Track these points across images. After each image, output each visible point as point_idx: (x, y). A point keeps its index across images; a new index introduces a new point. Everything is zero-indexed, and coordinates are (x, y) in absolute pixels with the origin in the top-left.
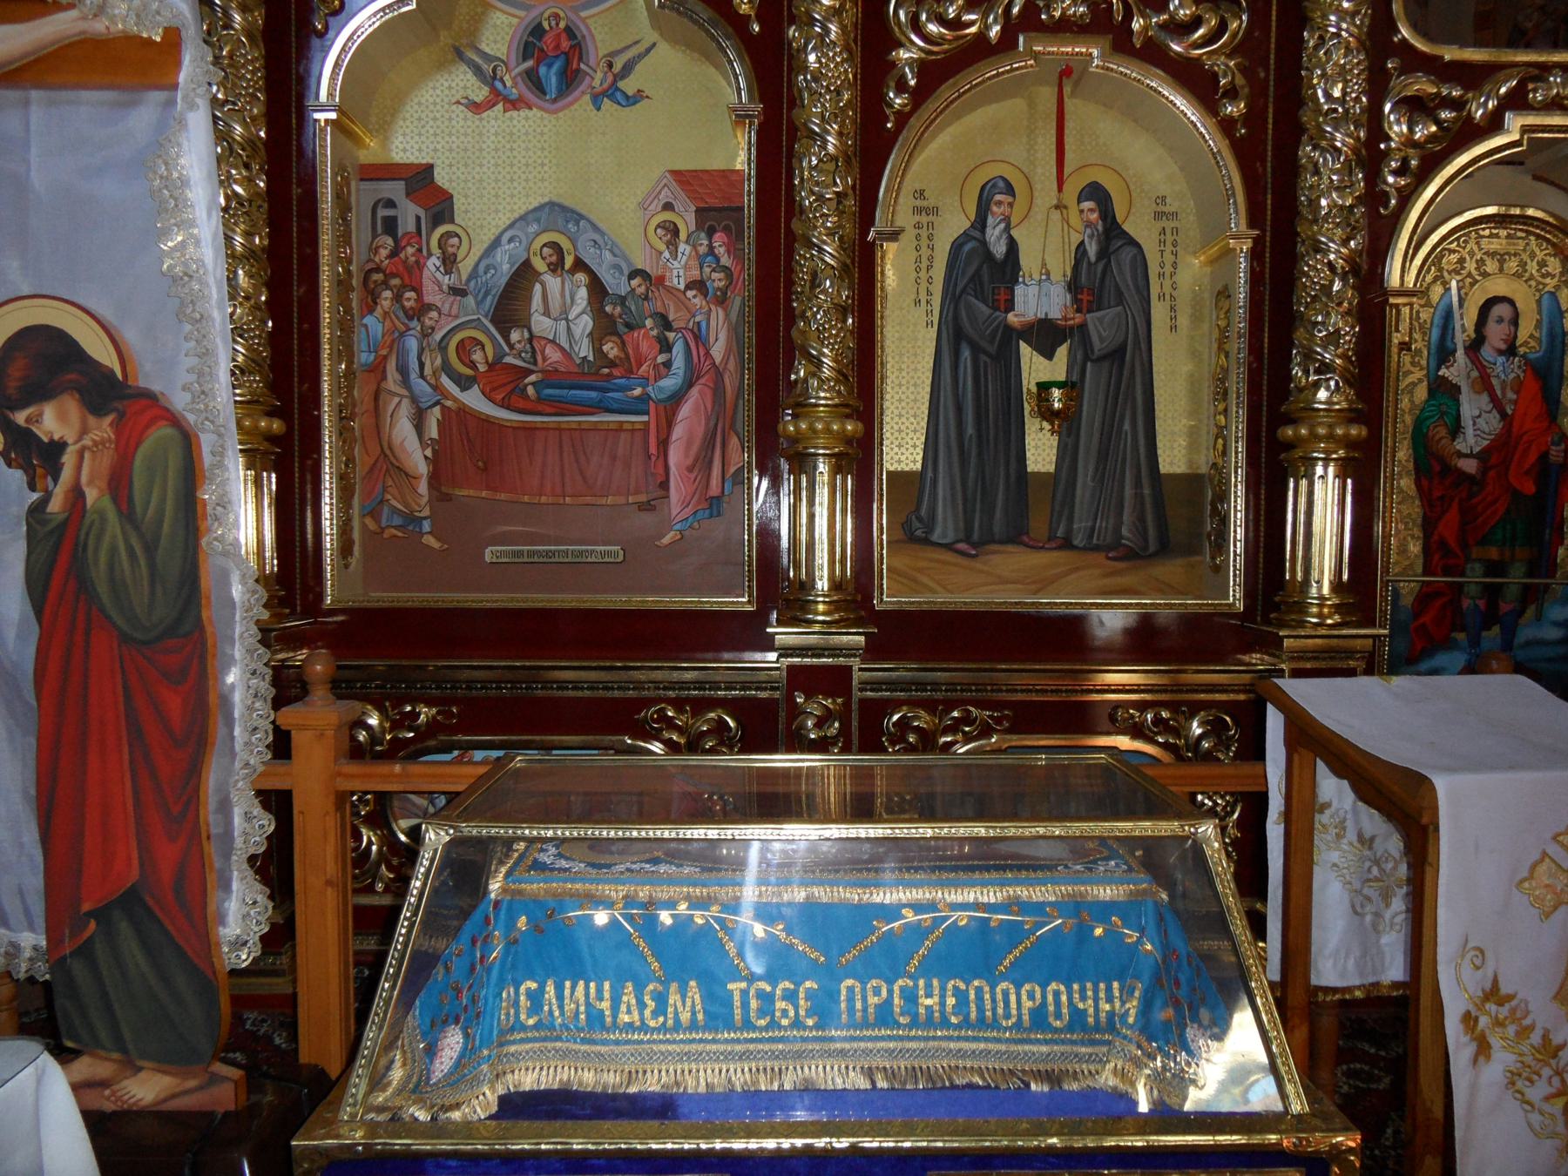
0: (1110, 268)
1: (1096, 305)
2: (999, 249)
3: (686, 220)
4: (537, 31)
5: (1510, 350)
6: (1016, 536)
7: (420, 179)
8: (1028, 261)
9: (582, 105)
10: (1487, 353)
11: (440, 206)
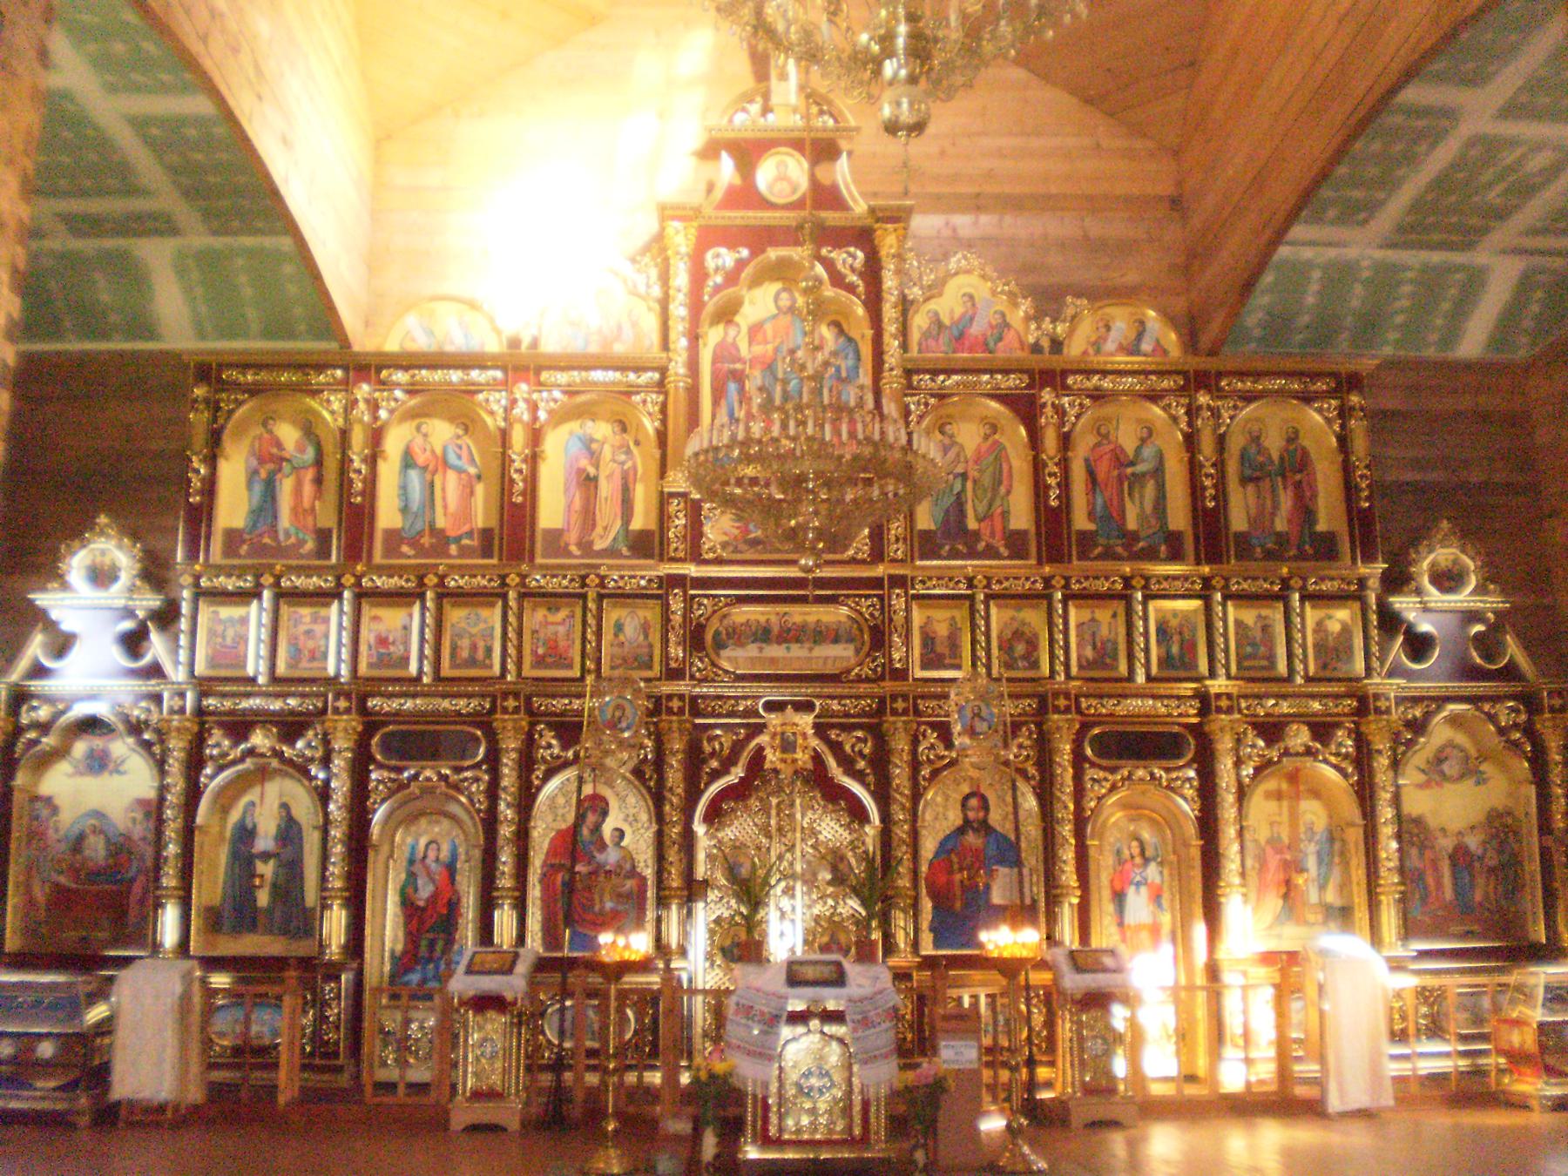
0: (289, 831)
1: (284, 846)
2: (250, 826)
3: (139, 816)
4: (92, 750)
5: (437, 860)
6: (253, 927)
7: (48, 801)
8: (261, 829)
9: (106, 774)
10: (428, 861)
11: (55, 810)
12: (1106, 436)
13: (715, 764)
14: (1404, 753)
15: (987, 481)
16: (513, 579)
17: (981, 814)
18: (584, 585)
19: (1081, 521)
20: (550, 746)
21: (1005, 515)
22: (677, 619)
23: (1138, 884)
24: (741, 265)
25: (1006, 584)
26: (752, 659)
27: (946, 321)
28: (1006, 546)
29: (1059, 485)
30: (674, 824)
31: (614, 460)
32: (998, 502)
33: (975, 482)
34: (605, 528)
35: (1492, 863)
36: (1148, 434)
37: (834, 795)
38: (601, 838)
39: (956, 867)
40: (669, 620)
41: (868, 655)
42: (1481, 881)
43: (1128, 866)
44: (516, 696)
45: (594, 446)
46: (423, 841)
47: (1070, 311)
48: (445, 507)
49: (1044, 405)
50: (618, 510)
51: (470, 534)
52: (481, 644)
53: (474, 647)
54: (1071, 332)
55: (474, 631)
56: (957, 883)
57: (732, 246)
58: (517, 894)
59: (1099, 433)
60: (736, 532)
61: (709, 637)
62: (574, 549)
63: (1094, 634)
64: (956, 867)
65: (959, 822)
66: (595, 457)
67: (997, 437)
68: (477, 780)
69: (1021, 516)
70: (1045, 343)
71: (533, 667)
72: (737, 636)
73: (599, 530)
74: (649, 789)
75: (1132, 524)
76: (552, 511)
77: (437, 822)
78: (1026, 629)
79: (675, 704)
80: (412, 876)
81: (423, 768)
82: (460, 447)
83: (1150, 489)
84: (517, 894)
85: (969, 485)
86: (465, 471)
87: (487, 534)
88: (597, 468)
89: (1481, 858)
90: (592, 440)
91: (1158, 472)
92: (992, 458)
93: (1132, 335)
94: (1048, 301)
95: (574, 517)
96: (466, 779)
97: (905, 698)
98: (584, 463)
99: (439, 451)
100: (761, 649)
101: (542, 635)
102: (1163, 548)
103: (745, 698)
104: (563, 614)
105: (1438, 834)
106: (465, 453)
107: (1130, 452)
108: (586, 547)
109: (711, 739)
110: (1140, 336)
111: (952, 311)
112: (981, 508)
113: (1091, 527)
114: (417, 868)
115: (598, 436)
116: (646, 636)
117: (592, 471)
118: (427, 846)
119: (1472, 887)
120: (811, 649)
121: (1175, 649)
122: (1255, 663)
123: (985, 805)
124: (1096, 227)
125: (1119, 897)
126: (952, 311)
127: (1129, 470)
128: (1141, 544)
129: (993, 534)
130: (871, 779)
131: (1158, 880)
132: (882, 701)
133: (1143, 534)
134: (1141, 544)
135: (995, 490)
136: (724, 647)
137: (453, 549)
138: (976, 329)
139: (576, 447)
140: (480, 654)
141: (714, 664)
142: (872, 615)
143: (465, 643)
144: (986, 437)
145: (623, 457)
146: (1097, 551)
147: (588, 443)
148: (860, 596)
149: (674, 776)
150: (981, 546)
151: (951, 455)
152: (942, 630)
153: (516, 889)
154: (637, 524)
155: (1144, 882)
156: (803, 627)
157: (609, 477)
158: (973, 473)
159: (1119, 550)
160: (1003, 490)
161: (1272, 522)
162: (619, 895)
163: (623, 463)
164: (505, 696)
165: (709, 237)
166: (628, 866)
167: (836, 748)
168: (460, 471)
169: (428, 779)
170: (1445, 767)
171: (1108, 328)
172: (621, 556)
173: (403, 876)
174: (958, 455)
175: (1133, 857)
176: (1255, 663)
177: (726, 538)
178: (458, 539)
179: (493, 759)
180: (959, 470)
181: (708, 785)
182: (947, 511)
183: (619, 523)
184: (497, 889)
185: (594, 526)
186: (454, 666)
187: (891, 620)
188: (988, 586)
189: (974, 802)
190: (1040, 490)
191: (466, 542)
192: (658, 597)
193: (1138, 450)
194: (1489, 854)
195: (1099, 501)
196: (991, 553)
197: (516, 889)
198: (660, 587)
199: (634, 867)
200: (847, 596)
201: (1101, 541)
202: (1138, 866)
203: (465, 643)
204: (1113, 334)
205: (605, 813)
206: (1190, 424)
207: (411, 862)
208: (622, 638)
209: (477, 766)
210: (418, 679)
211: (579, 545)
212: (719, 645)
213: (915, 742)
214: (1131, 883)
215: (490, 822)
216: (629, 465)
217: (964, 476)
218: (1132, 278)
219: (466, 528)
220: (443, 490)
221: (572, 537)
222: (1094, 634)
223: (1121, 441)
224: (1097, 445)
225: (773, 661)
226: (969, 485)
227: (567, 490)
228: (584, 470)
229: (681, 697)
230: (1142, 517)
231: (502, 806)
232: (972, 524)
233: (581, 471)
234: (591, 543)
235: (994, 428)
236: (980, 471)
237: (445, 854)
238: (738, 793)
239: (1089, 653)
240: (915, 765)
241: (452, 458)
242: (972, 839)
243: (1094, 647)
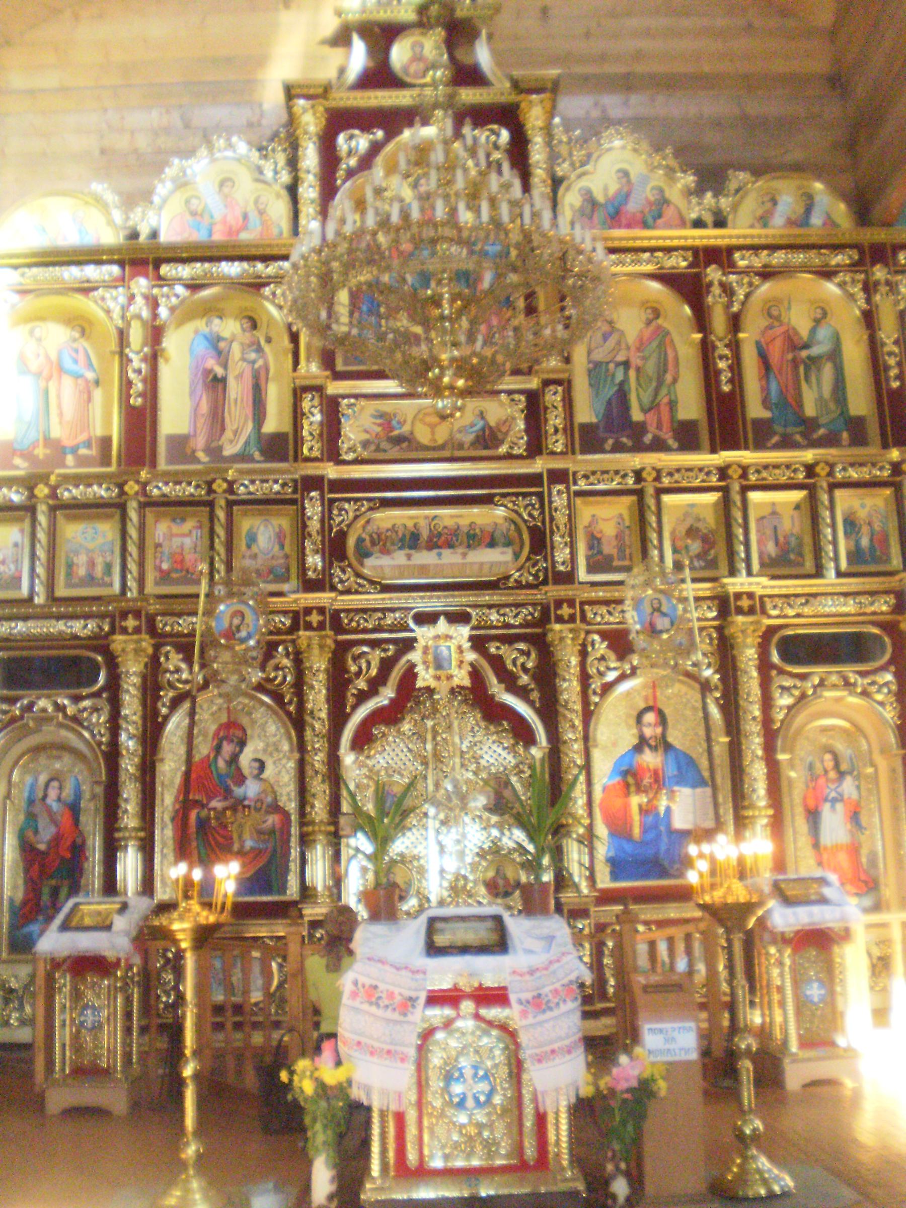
5: (59, 799)
12: (778, 318)
13: (362, 684)
15: (650, 368)
16: (132, 488)
17: (659, 730)
18: (210, 491)
19: (755, 410)
20: (178, 670)
21: (672, 405)
22: (314, 525)
23: (834, 801)
24: (376, 148)
25: (677, 476)
26: (399, 566)
27: (600, 198)
28: (676, 439)
29: (731, 368)
30: (316, 751)
31: (243, 359)
32: (664, 391)
33: (638, 370)
34: (235, 432)
36: (821, 316)
37: (494, 713)
38: (239, 769)
40: (305, 526)
41: (528, 559)
43: (822, 781)
44: (137, 614)
45: (222, 345)
46: (43, 779)
47: (732, 185)
48: (61, 415)
49: (710, 284)
50: (249, 411)
51: (88, 444)
52: (99, 560)
53: (92, 564)
54: (735, 207)
55: (91, 545)
56: (635, 810)
57: (366, 128)
58: (142, 834)
59: (770, 315)
60: (379, 429)
61: (351, 542)
62: (201, 455)
63: (775, 528)
65: (635, 741)
66: (222, 357)
67: (660, 321)
68: (95, 709)
69: (690, 405)
70: (708, 218)
71: (157, 583)
72: (382, 542)
73: (228, 434)
74: (288, 714)
75: (810, 410)
76: (176, 415)
77: (59, 758)
78: (700, 525)
79: (315, 618)
80: (31, 817)
81: (39, 698)
82: (77, 351)
83: (828, 371)
84: (142, 834)
85: (632, 373)
86: (82, 376)
87: (106, 442)
88: (225, 366)
90: (219, 339)
91: (835, 356)
92: (654, 344)
93: (801, 210)
94: (711, 178)
95: (201, 421)
96: (85, 709)
97: (571, 603)
98: (211, 363)
99: (53, 356)
100: (409, 557)
101: (166, 550)
102: (845, 435)
103: (393, 610)
104: (189, 524)
106: (81, 357)
107: (804, 333)
108: (215, 452)
109: (356, 659)
110: (809, 210)
111: (606, 189)
112: (646, 400)
113: (766, 414)
114: (38, 808)
115: (226, 334)
116: (282, 546)
117: (219, 371)
118: (47, 786)
120: (464, 555)
121: (865, 542)
123: (662, 719)
124: (754, 107)
125: (813, 816)
126: (606, 189)
127: (804, 354)
128: (822, 431)
129: (659, 427)
130: (535, 695)
131: (855, 795)
132: (545, 611)
133: (823, 420)
134: (822, 431)
135: (660, 382)
136: (368, 555)
137: (70, 459)
138: (632, 207)
139: (202, 346)
140: (99, 570)
141: (358, 575)
142: (530, 515)
143: (81, 560)
144: (649, 323)
145: (253, 356)
146: (775, 439)
147: (215, 342)
148: (517, 495)
149: (318, 698)
150: (648, 438)
151: (612, 342)
152: (609, 530)
153: (142, 829)
154: (270, 426)
155: (840, 799)
156: (455, 532)
157: (240, 377)
158: (636, 361)
159: (798, 438)
160: (669, 377)
162: (260, 832)
163: (253, 362)
164: (124, 615)
165: (340, 120)
166: (269, 799)
167: (497, 663)
168: (77, 376)
169: (44, 710)
171: (774, 202)
172: (250, 459)
173: (22, 817)
174: (619, 343)
177: (366, 436)
178: (74, 450)
179: (114, 688)
180: (621, 358)
181: (355, 707)
182: (609, 403)
183: (250, 426)
184: (119, 830)
185: (223, 429)
186: (69, 585)
187: (552, 519)
188: (658, 479)
189: (650, 717)
190: (709, 374)
191: (83, 451)
192: (293, 502)
193: (813, 331)
195: (774, 386)
196: (659, 446)
197: (142, 829)
198: (295, 491)
199: (275, 800)
200: (504, 496)
201: (778, 428)
202: (833, 781)
203: (81, 560)
204: (780, 208)
205: (242, 744)
206: (868, 300)
207: (31, 802)
208: (254, 549)
209: (97, 695)
210: (30, 599)
211: (208, 450)
212: (363, 554)
213: (583, 654)
214: (826, 800)
215: (113, 755)
216: (260, 363)
217: (626, 364)
218: (796, 155)
219: (83, 437)
220: (59, 397)
221: (200, 442)
223: (794, 322)
224: (770, 327)
225: (423, 570)
226: (632, 373)
227: (192, 393)
228: (210, 371)
229: (321, 610)
230: (820, 400)
231: (123, 737)
232: (637, 415)
233: (208, 372)
234: (220, 449)
235: (657, 313)
236: (644, 358)
237: (68, 793)
238: (390, 716)
239: (771, 548)
240: (585, 678)
241: (68, 364)
242: (650, 759)
243: (777, 543)
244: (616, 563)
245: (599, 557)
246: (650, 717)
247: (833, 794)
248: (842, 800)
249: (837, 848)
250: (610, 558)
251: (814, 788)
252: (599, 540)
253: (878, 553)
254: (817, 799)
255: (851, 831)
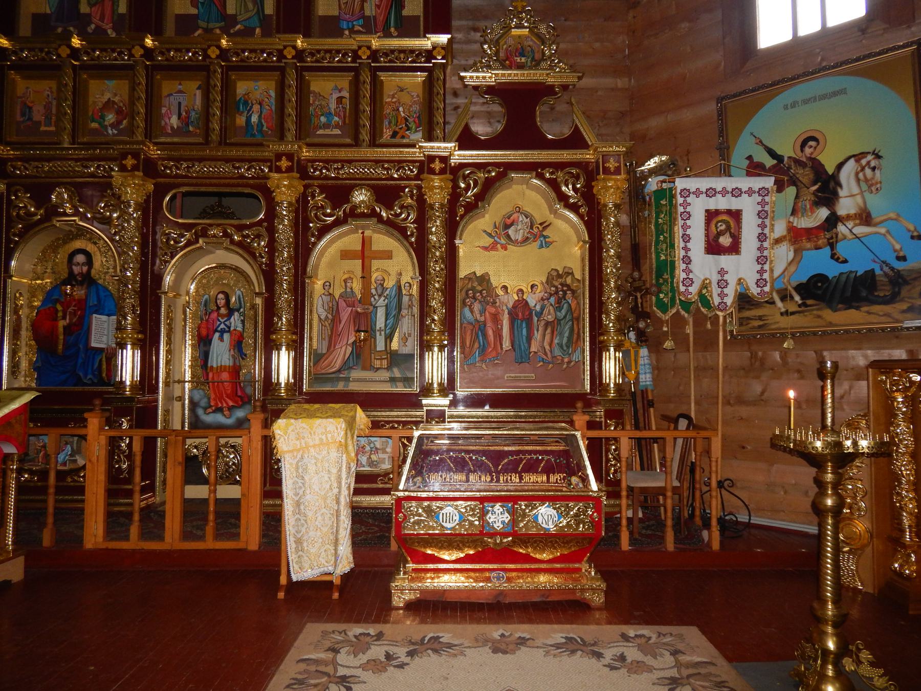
14: (462, 217)
17: (85, 269)
23: (222, 332)
35: (550, 318)
39: (60, 314)
42: (537, 335)
43: (215, 315)
56: (61, 330)
63: (180, 104)
64: (60, 314)
78: (116, 99)
89: (540, 314)
102: (258, 31)
105: (500, 292)
119: (529, 338)
121: (254, 119)
122: (328, 132)
129: (102, 19)
131: (240, 329)
133: (239, 18)
134: (238, 27)
161: (362, 8)
170: (511, 231)
175: (219, 308)
176: (328, 132)
194: (546, 311)
201: (202, 24)
202: (223, 316)
222: (180, 104)
239: (174, 121)
244: (43, 128)
245: (29, 123)
246: (80, 258)
247: (222, 326)
248: (229, 331)
249: (222, 369)
250: (39, 123)
251: (207, 321)
252: (30, 108)
253: (265, 128)
254: (208, 329)
255: (233, 356)
